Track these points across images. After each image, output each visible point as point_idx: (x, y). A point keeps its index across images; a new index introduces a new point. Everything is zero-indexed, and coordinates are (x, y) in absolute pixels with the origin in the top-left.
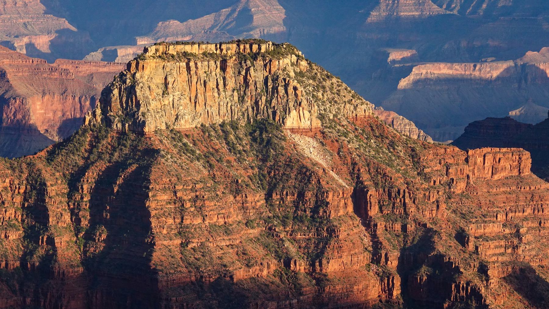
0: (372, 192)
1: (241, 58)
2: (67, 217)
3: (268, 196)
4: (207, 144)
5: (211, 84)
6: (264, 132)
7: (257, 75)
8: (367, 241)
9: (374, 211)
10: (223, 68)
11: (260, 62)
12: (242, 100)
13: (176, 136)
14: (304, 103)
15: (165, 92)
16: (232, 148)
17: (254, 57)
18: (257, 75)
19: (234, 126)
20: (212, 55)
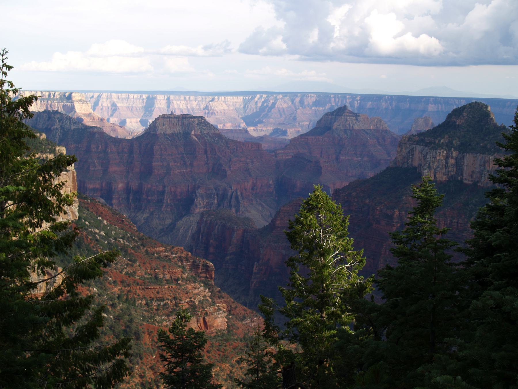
0: (208, 148)
1: (183, 118)
2: (138, 152)
3: (184, 149)
4: (173, 137)
5: (175, 124)
6: (187, 134)
7: (186, 122)
8: (206, 160)
9: (209, 153)
10: (178, 121)
11: (187, 119)
12: (182, 128)
13: (165, 135)
14: (196, 128)
15: (164, 125)
16: (178, 138)
17: (185, 118)
18: (186, 122)
19: (180, 133)
20: (176, 118)
